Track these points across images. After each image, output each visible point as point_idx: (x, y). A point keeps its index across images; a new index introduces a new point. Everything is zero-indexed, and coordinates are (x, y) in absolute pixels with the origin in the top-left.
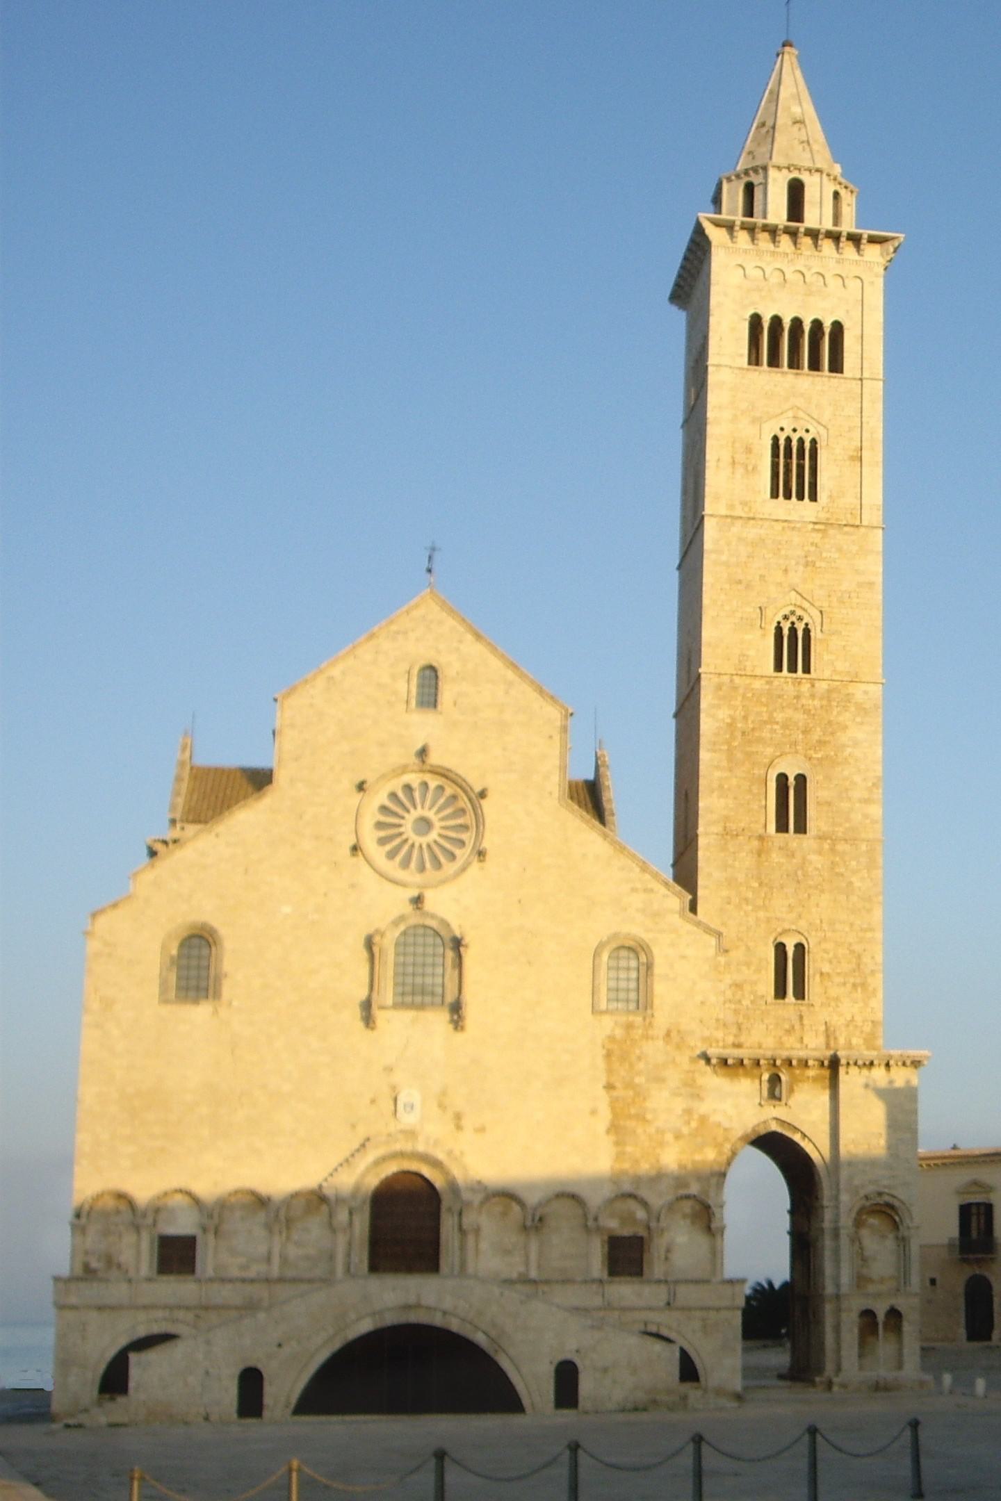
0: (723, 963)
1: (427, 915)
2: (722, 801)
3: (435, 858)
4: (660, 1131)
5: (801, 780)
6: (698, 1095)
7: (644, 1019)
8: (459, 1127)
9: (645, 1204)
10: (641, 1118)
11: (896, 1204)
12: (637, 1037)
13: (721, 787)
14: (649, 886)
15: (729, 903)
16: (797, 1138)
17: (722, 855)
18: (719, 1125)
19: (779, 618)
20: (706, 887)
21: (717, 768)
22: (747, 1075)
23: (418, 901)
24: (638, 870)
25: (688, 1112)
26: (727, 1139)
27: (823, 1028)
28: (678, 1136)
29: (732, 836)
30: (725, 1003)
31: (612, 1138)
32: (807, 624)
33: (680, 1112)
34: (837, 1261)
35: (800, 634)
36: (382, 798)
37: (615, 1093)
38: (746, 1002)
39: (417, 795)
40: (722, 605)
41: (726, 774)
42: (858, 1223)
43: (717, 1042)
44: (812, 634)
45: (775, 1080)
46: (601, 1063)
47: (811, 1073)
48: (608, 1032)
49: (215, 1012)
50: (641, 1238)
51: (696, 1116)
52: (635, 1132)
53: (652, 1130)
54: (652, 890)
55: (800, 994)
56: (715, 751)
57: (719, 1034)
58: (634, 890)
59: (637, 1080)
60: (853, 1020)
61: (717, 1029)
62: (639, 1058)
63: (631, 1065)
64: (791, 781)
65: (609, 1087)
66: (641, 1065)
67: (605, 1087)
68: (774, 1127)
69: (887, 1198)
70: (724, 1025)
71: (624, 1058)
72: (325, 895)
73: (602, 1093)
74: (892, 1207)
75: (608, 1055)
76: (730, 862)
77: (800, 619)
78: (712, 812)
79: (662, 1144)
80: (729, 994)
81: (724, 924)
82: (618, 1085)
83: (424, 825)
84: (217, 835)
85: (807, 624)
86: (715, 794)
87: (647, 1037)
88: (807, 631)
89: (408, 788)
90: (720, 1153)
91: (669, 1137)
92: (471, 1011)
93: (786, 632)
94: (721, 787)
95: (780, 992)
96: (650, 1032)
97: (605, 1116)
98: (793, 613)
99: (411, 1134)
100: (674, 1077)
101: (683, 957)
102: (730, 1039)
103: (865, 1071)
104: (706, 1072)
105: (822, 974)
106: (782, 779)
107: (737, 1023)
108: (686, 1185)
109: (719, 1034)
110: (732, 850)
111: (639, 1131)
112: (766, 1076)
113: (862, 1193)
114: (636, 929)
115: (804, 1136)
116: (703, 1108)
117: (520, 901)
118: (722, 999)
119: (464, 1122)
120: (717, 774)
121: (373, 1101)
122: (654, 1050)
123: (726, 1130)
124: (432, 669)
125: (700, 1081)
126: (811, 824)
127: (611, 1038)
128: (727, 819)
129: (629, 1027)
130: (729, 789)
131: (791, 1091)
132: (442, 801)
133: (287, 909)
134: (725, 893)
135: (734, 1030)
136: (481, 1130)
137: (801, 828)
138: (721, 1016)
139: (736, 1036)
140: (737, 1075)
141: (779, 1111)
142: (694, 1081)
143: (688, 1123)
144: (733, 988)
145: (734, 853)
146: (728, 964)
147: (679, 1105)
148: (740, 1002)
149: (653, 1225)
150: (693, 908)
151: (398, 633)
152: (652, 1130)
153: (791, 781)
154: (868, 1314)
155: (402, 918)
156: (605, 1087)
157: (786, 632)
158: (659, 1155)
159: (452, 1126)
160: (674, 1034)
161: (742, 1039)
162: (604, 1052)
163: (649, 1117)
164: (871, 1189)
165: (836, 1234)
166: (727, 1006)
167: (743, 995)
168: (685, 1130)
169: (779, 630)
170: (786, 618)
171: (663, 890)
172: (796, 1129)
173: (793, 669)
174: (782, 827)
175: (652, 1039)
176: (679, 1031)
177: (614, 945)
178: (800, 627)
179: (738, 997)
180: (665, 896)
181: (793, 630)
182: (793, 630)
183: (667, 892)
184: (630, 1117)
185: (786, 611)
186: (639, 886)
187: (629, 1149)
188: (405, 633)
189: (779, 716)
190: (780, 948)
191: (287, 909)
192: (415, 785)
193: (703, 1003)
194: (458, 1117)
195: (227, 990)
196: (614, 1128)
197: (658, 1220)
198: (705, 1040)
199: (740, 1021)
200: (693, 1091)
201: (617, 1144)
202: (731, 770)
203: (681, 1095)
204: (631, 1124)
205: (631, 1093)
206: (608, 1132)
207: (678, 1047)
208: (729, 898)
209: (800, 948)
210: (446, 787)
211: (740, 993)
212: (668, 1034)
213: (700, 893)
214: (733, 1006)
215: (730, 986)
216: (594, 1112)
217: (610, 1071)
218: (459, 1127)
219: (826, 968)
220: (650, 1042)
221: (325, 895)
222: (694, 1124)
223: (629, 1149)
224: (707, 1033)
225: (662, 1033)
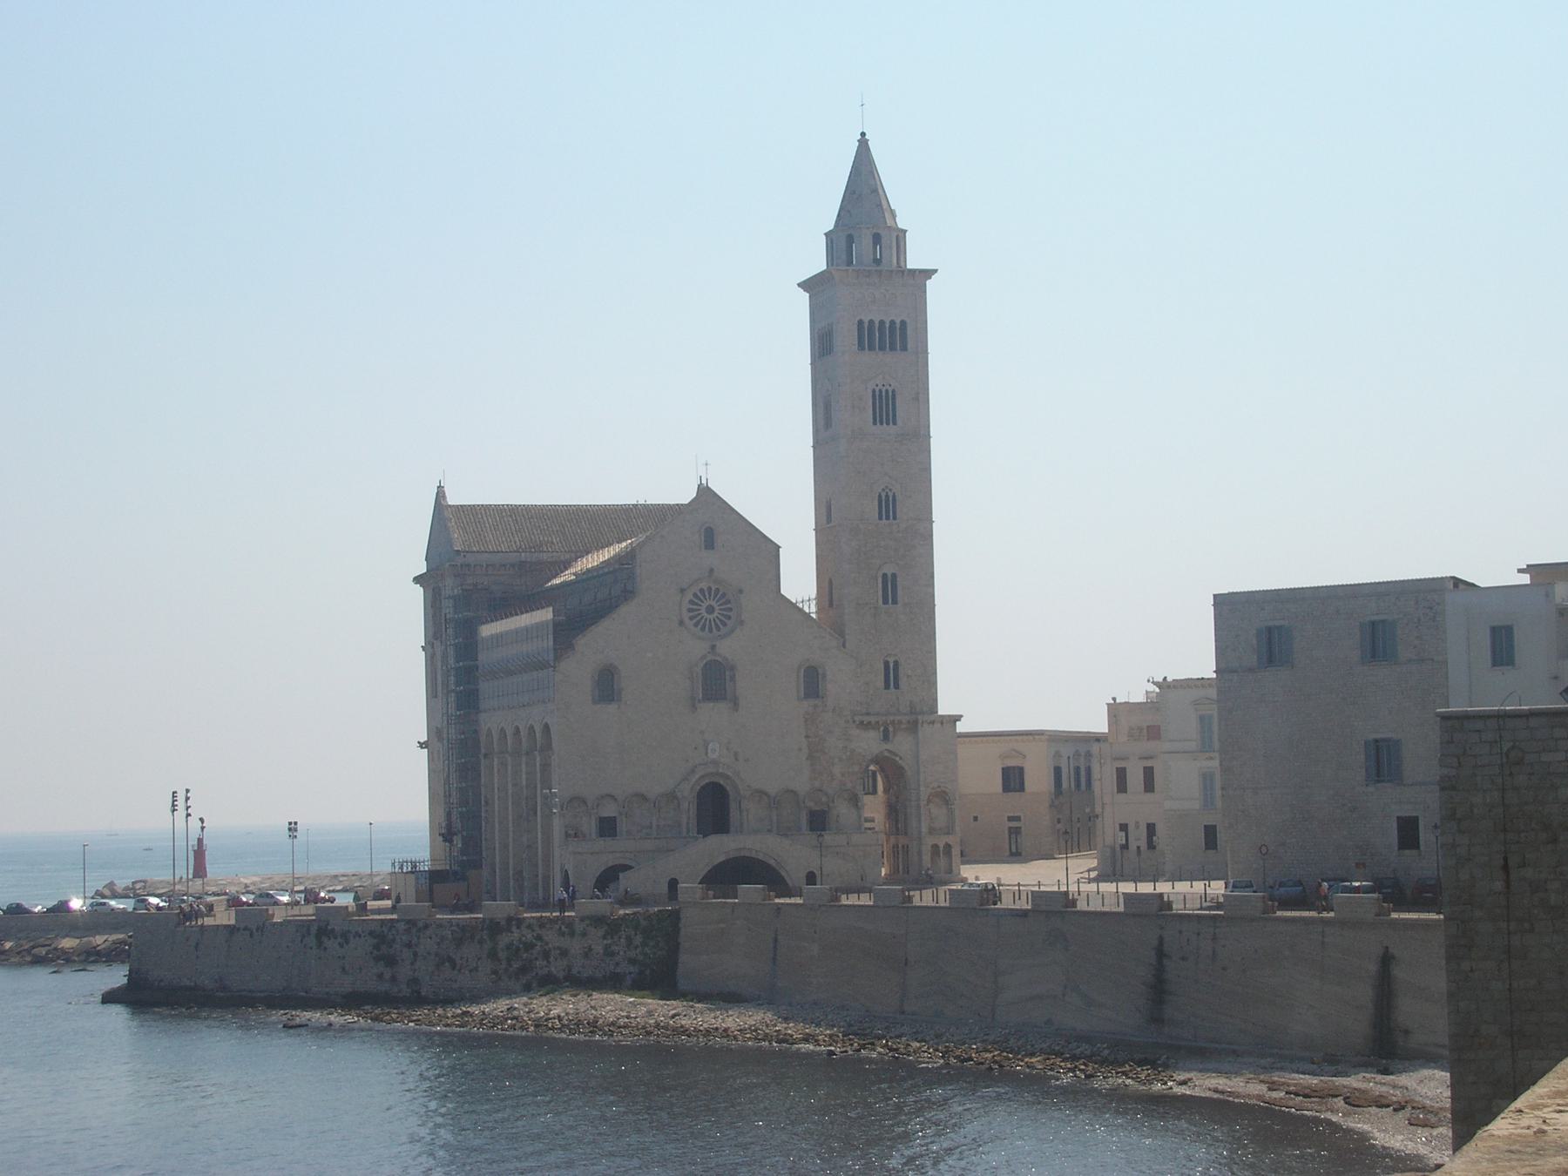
5: (894, 576)
8: (737, 759)
9: (826, 794)
11: (947, 790)
16: (898, 759)
19: (880, 491)
22: (873, 729)
23: (713, 647)
27: (908, 703)
32: (894, 494)
34: (919, 821)
35: (891, 499)
36: (689, 596)
38: (871, 692)
42: (929, 801)
44: (897, 498)
45: (886, 732)
47: (903, 726)
49: (619, 707)
50: (825, 811)
55: (897, 687)
60: (923, 699)
62: (821, 722)
64: (889, 576)
65: (807, 737)
68: (886, 754)
69: (944, 789)
73: (804, 739)
74: (944, 792)
75: (806, 721)
77: (890, 490)
85: (894, 494)
88: (894, 496)
89: (702, 591)
91: (836, 760)
93: (884, 498)
95: (887, 686)
98: (887, 487)
99: (715, 763)
103: (931, 725)
105: (908, 676)
106: (885, 575)
112: (882, 729)
113: (931, 786)
115: (901, 758)
121: (696, 748)
123: (864, 756)
124: (711, 528)
126: (899, 599)
131: (894, 736)
137: (895, 602)
141: (889, 746)
149: (831, 805)
150: (844, 646)
153: (889, 576)
154: (935, 847)
155: (704, 657)
157: (884, 498)
164: (936, 785)
165: (919, 807)
168: (844, 757)
169: (880, 496)
170: (883, 490)
172: (897, 755)
173: (888, 518)
174: (885, 602)
178: (891, 494)
181: (887, 496)
182: (887, 496)
185: (883, 487)
189: (883, 543)
190: (886, 664)
194: (736, 754)
197: (833, 801)
205: (817, 739)
209: (896, 663)
212: (834, 710)
213: (847, 637)
216: (800, 750)
218: (737, 759)
219: (910, 672)
222: (848, 753)
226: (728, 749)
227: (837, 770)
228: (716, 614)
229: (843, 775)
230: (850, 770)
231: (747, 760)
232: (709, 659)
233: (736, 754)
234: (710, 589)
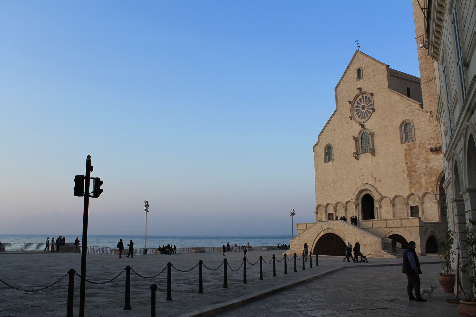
0: (431, 120)
1: (366, 129)
2: (426, 72)
3: (367, 115)
4: (420, 174)
6: (429, 161)
7: (413, 143)
8: (376, 181)
10: (415, 171)
12: (412, 148)
13: (425, 68)
14: (411, 104)
15: (431, 102)
17: (428, 88)
18: (435, 169)
20: (425, 99)
21: (423, 63)
24: (407, 101)
25: (426, 167)
26: (438, 173)
28: (425, 175)
29: (430, 81)
30: (433, 132)
31: (408, 178)
33: (425, 167)
37: (408, 165)
39: (362, 100)
40: (419, 17)
41: (426, 64)
43: (432, 144)
46: (404, 157)
48: (405, 149)
51: (429, 168)
52: (414, 176)
53: (418, 174)
54: (411, 105)
56: (422, 59)
57: (433, 142)
58: (407, 107)
59: (413, 160)
61: (432, 140)
62: (413, 154)
63: (411, 157)
65: (406, 164)
66: (414, 156)
67: (405, 164)
70: (434, 138)
71: (409, 155)
72: (347, 130)
73: (405, 165)
75: (405, 155)
76: (430, 89)
78: (424, 77)
79: (421, 178)
80: (434, 129)
81: (431, 108)
82: (408, 162)
83: (363, 107)
84: (330, 124)
86: (424, 72)
87: (414, 148)
89: (360, 100)
90: (436, 178)
91: (422, 175)
92: (377, 151)
94: (425, 68)
96: (415, 146)
97: (406, 172)
100: (422, 158)
101: (421, 122)
102: (436, 142)
104: (430, 154)
107: (437, 137)
108: (428, 189)
109: (433, 142)
110: (430, 86)
111: (415, 175)
114: (408, 118)
116: (430, 165)
117: (382, 119)
118: (432, 131)
119: (377, 180)
120: (424, 65)
121: (359, 177)
122: (416, 151)
123: (437, 170)
125: (429, 157)
127: (406, 150)
128: (428, 77)
129: (410, 146)
130: (427, 68)
132: (364, 99)
133: (341, 136)
134: (430, 99)
135: (436, 140)
136: (380, 181)
138: (433, 136)
139: (437, 141)
140: (439, 153)
142: (427, 157)
143: (427, 170)
144: (435, 127)
145: (431, 86)
146: (433, 120)
147: (424, 165)
148: (437, 131)
150: (422, 106)
151: (353, 64)
152: (418, 174)
155: (360, 132)
156: (405, 164)
158: (420, 181)
159: (374, 181)
160: (421, 145)
161: (439, 142)
162: (404, 154)
163: (417, 170)
166: (434, 132)
167: (438, 128)
168: (426, 173)
171: (414, 104)
175: (416, 148)
176: (422, 144)
177: (404, 124)
179: (437, 129)
180: (414, 106)
183: (415, 104)
184: (412, 171)
186: (408, 105)
187: (413, 180)
188: (354, 63)
191: (341, 136)
192: (361, 98)
193: (427, 134)
194: (375, 178)
195: (335, 158)
196: (409, 175)
198: (429, 144)
199: (438, 136)
200: (427, 161)
201: (410, 179)
202: (427, 62)
203: (424, 162)
204: (412, 173)
205: (412, 164)
206: (407, 177)
207: (422, 148)
208: (431, 100)
210: (367, 96)
211: (437, 128)
212: (419, 146)
213: (424, 101)
214: (436, 132)
215: (434, 126)
216: (403, 172)
217: (406, 159)
218: (376, 181)
220: (415, 149)
221: (347, 130)
222: (428, 170)
223: (413, 180)
224: (429, 142)
225: (418, 145)
226: (372, 176)
227: (423, 181)
228: (366, 109)
229: (427, 184)
230: (430, 180)
231: (380, 181)
232: (363, 132)
233: (375, 178)
234: (363, 98)
